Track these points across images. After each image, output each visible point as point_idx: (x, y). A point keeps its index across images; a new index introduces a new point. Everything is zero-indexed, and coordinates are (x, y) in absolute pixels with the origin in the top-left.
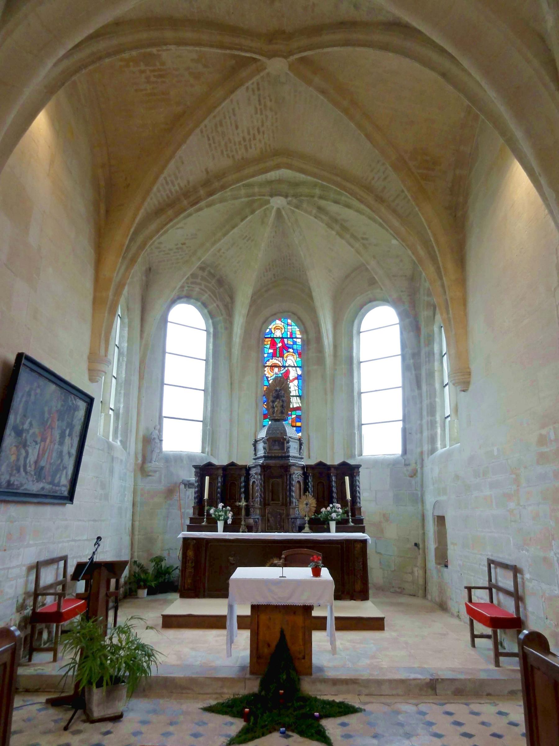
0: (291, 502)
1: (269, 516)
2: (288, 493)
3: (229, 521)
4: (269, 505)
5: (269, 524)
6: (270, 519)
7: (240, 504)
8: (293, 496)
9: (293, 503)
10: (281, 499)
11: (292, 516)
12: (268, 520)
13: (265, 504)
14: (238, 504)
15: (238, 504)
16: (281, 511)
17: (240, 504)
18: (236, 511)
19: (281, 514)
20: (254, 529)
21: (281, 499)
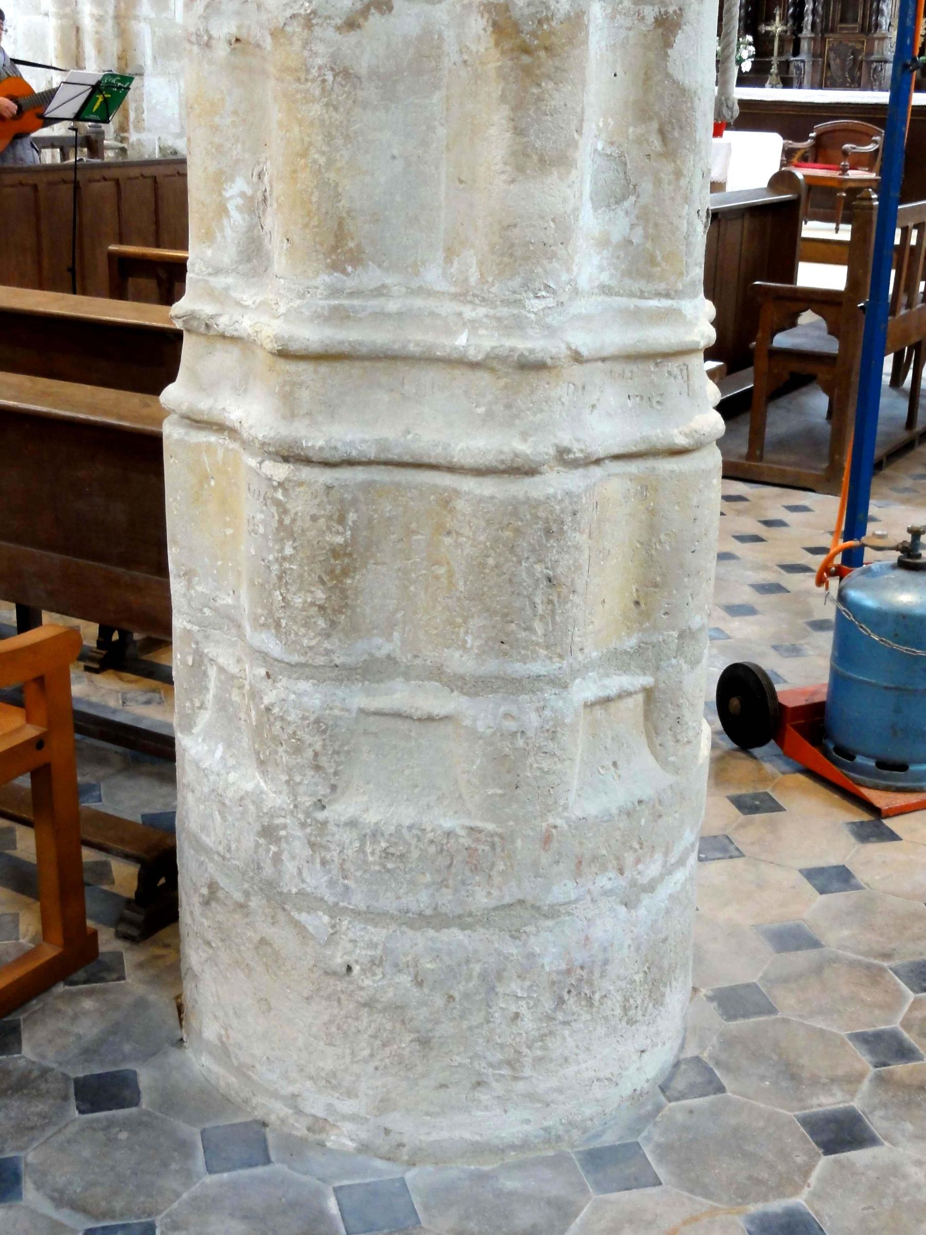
0: (878, 26)
1: (832, 55)
2: (875, 5)
3: (747, 66)
4: (833, 30)
5: (829, 74)
6: (832, 63)
7: (769, 28)
8: (882, 11)
9: (881, 27)
10: (860, 20)
11: (875, 57)
12: (829, 65)
13: (824, 29)
14: (764, 28)
15: (764, 28)
16: (858, 46)
17: (769, 28)
18: (762, 46)
19: (855, 52)
20: (795, 83)
21: (860, 20)
